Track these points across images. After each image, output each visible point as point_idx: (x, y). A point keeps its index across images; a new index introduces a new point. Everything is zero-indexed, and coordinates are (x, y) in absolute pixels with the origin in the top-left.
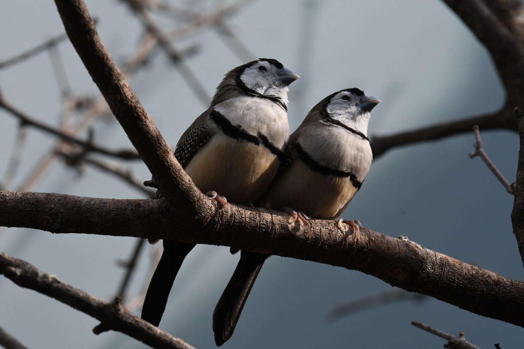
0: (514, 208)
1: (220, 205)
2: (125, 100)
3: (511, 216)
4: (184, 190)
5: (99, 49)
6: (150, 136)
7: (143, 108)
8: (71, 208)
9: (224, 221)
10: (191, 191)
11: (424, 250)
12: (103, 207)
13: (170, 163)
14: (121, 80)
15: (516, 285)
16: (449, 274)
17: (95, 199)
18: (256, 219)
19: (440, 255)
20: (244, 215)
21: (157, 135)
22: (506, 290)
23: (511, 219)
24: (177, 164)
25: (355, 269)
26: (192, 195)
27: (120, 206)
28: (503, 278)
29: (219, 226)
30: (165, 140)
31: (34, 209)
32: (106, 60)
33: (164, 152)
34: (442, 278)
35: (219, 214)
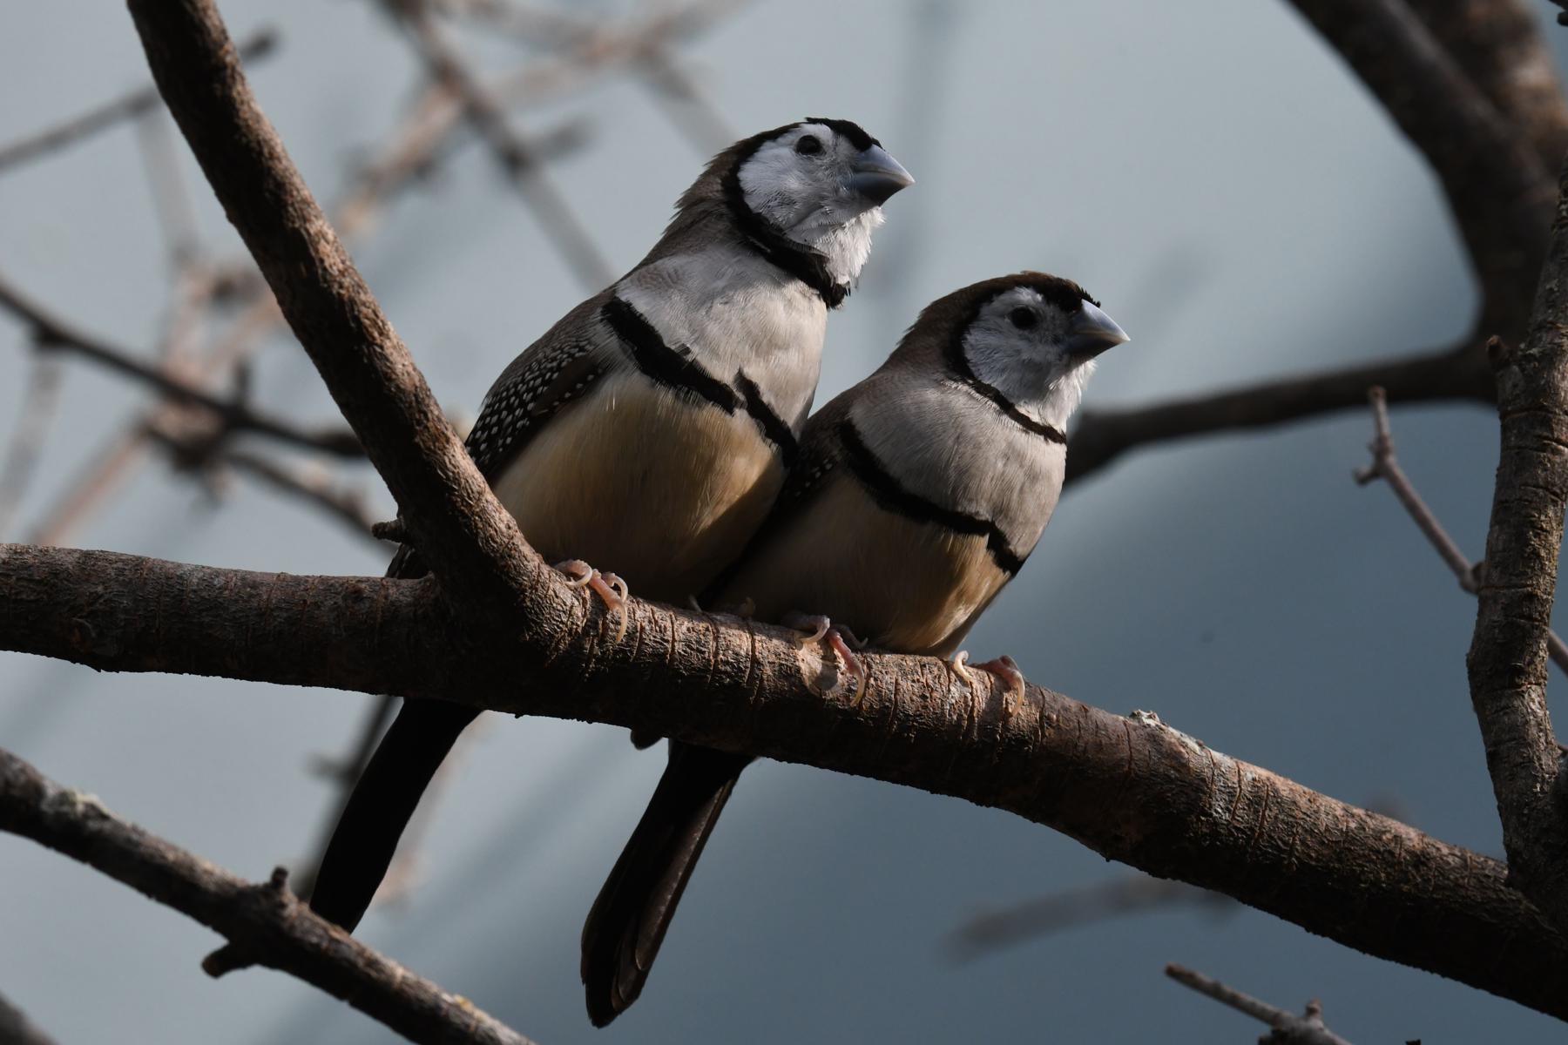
0: (1478, 637)
1: (600, 605)
2: (321, 280)
3: (1467, 660)
4: (492, 555)
5: (248, 126)
6: (393, 389)
7: (375, 305)
8: (156, 595)
9: (608, 650)
10: (514, 558)
11: (1204, 755)
12: (251, 596)
13: (453, 472)
14: (313, 218)
15: (1476, 868)
16: (1278, 827)
17: (226, 573)
18: (704, 646)
19: (1252, 772)
20: (669, 633)
21: (416, 387)
22: (1446, 882)
23: (1466, 670)
24: (473, 476)
25: (997, 805)
26: (515, 569)
27: (301, 596)
28: (1437, 846)
29: (595, 663)
30: (439, 402)
31: (45, 597)
32: (266, 159)
34: (1257, 840)
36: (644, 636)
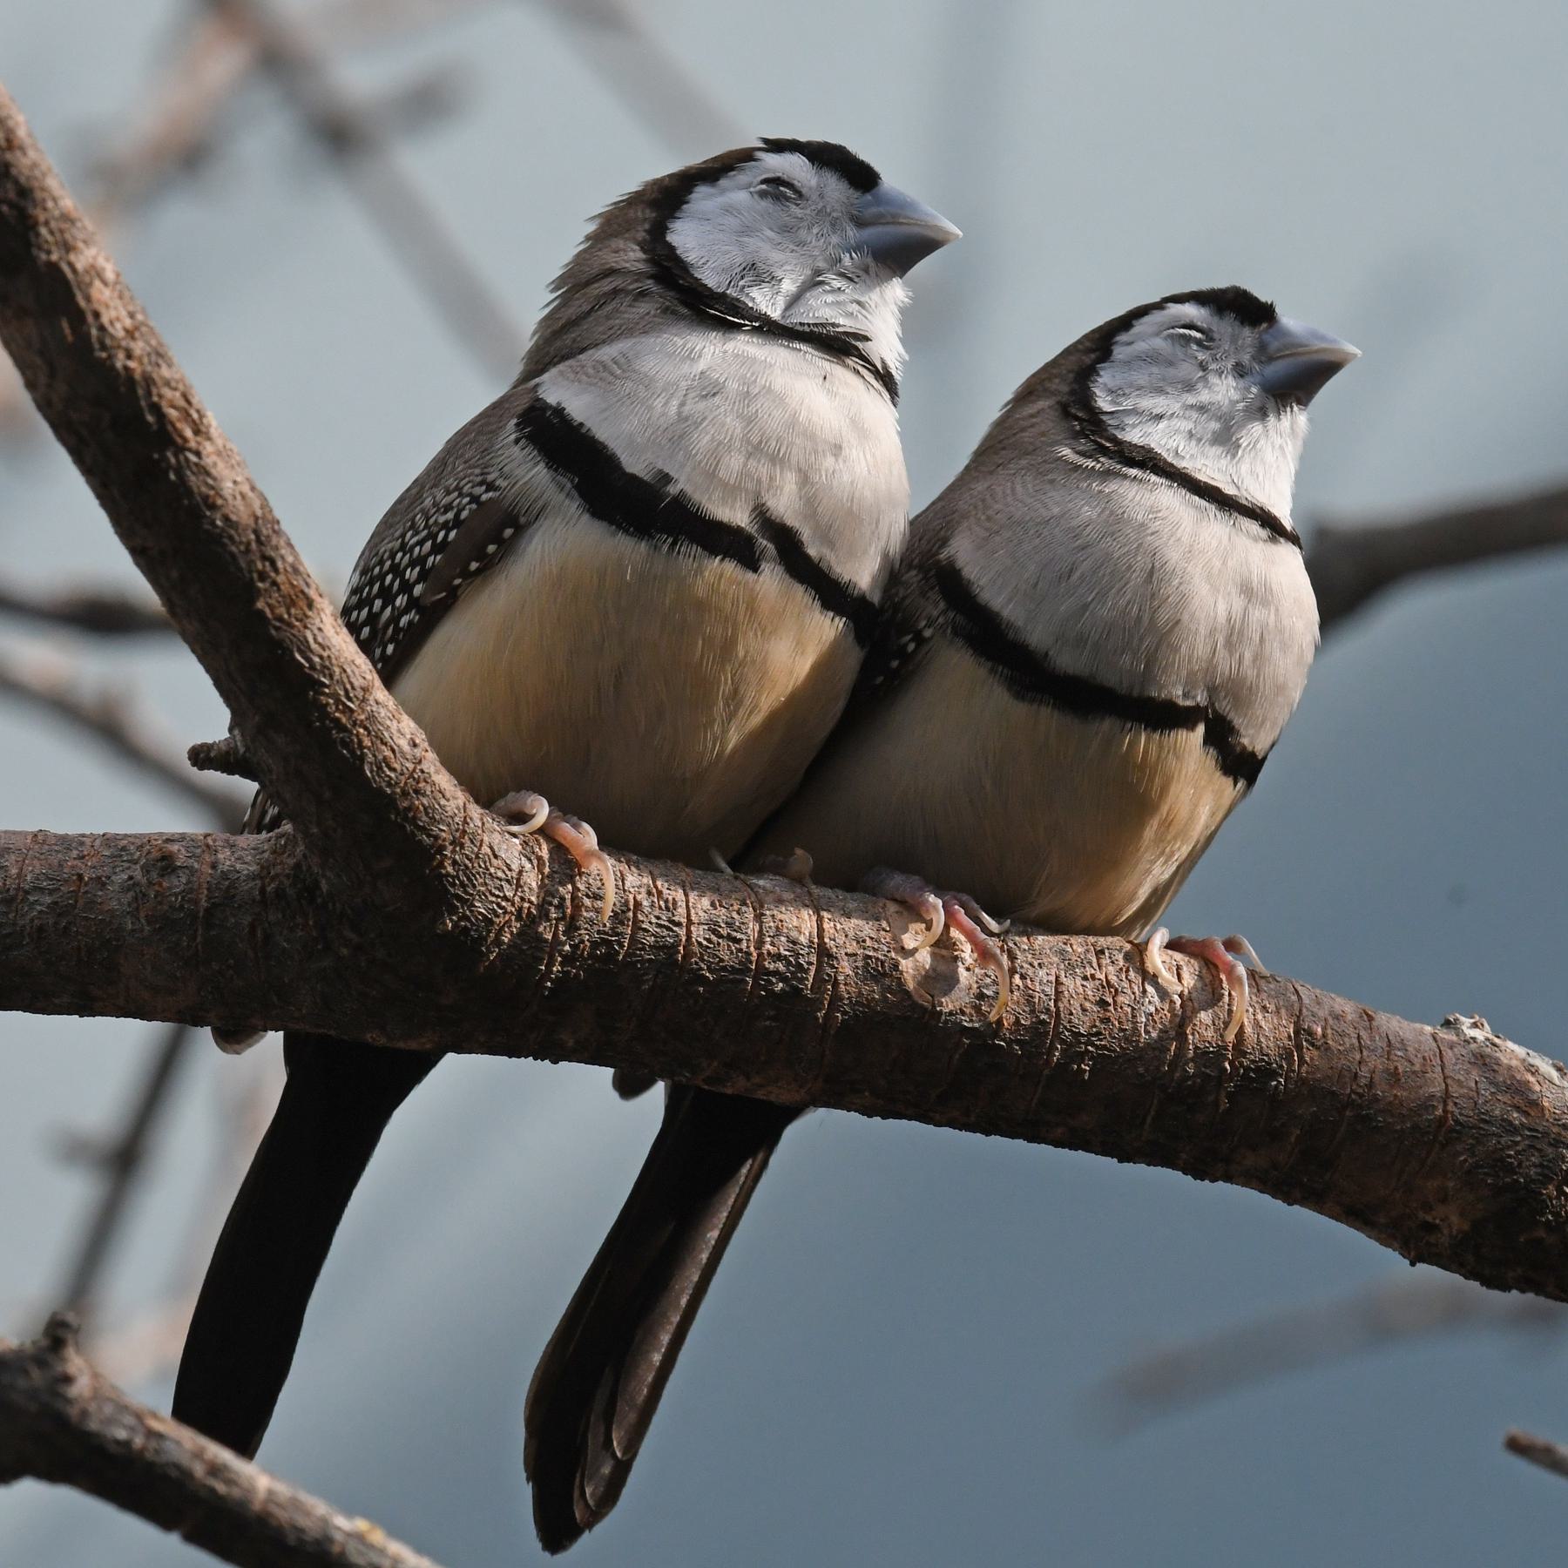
1: (565, 864)
2: (97, 346)
4: (388, 791)
6: (219, 523)
7: (185, 385)
9: (582, 942)
10: (424, 795)
13: (321, 657)
14: (80, 245)
18: (739, 930)
20: (682, 910)
21: (256, 518)
24: (353, 662)
27: (73, 867)
29: (561, 964)
30: (293, 542)
33: (290, 603)
35: (561, 906)
36: (640, 917)
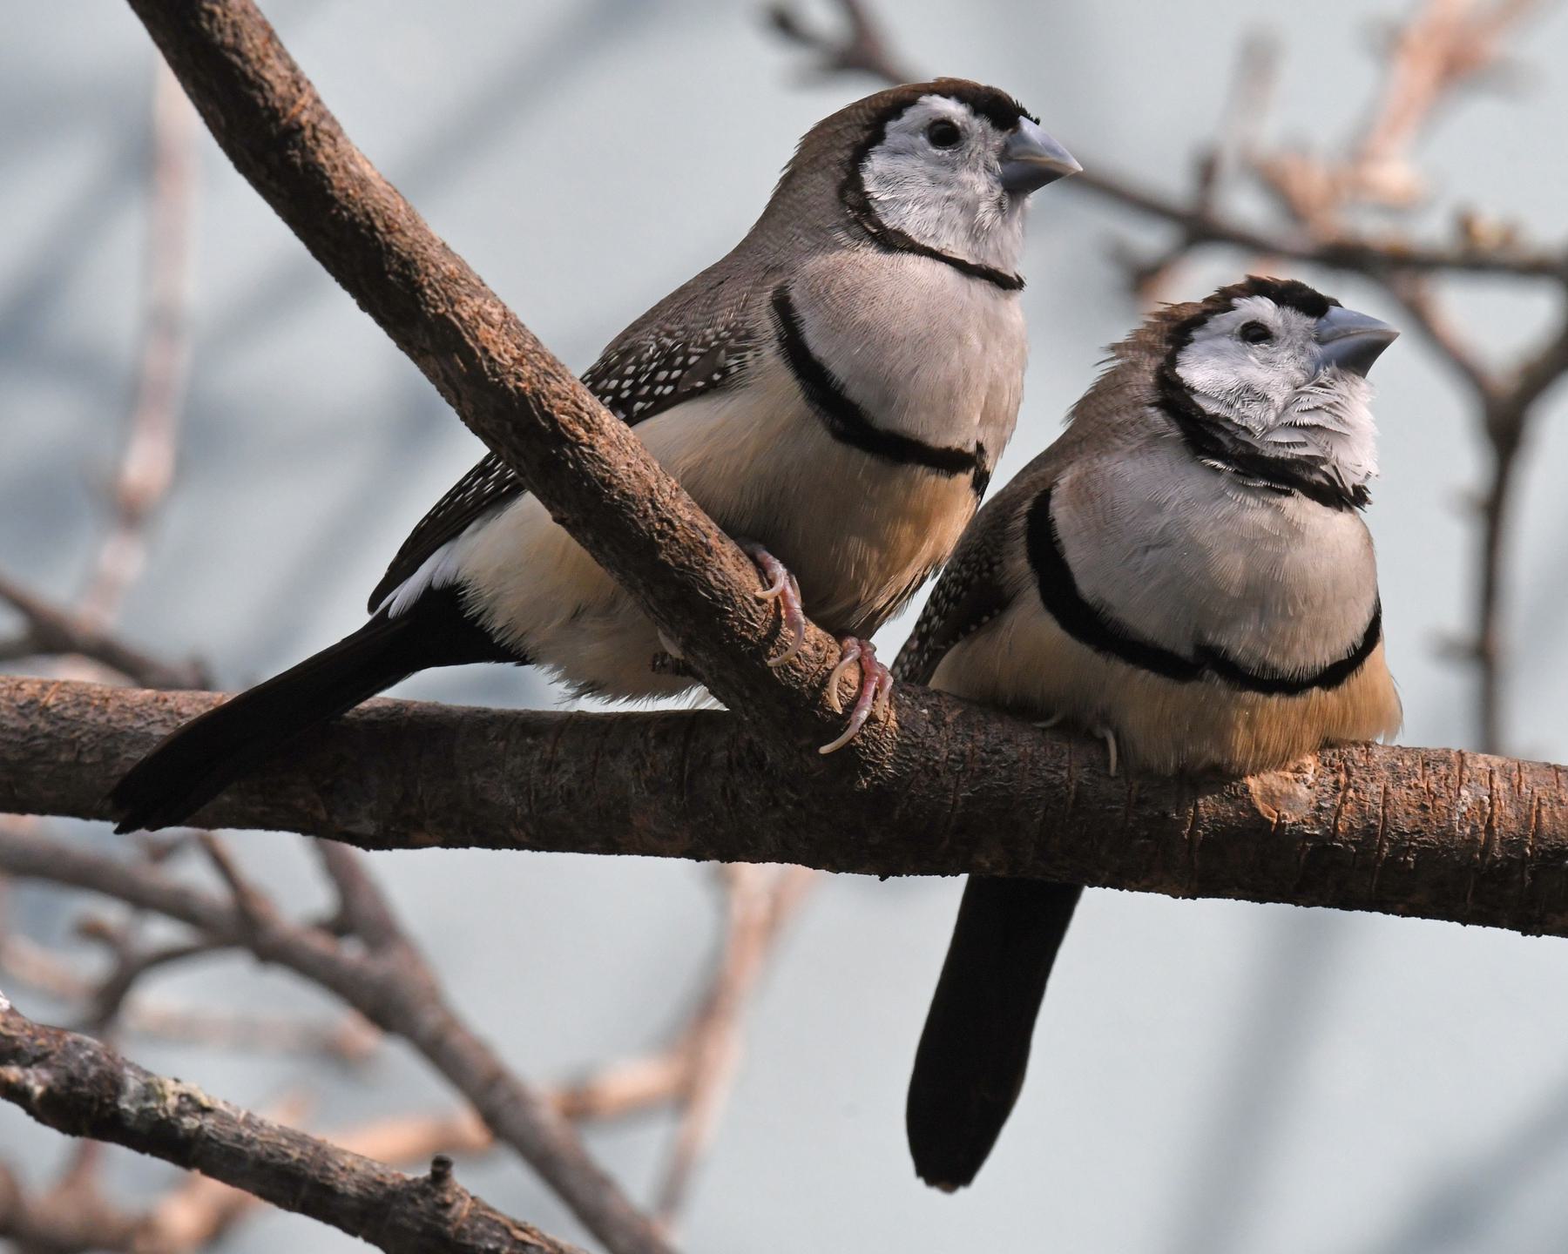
2: (489, 374)
5: (348, 196)
6: (616, 497)
13: (722, 591)
14: (464, 298)
32: (381, 233)
33: (690, 552)
